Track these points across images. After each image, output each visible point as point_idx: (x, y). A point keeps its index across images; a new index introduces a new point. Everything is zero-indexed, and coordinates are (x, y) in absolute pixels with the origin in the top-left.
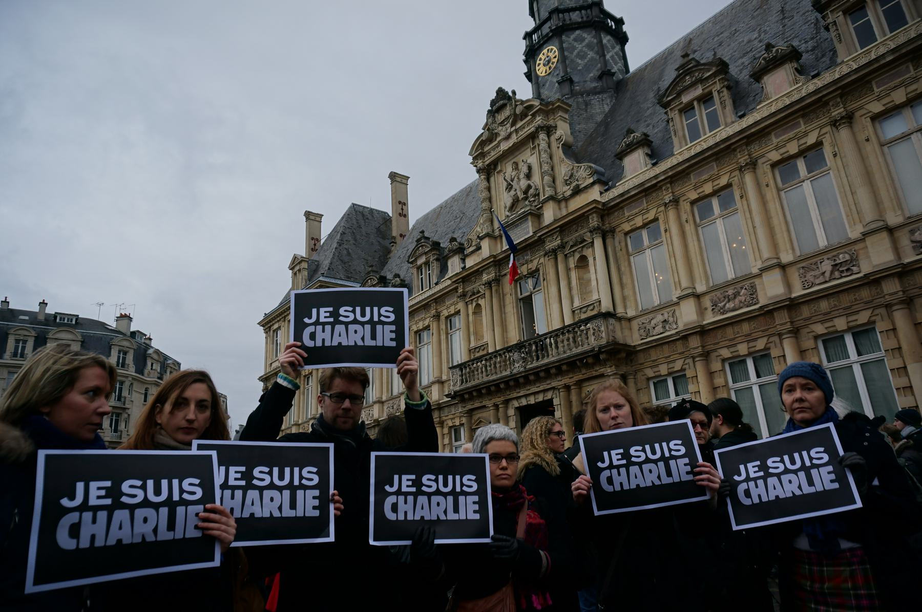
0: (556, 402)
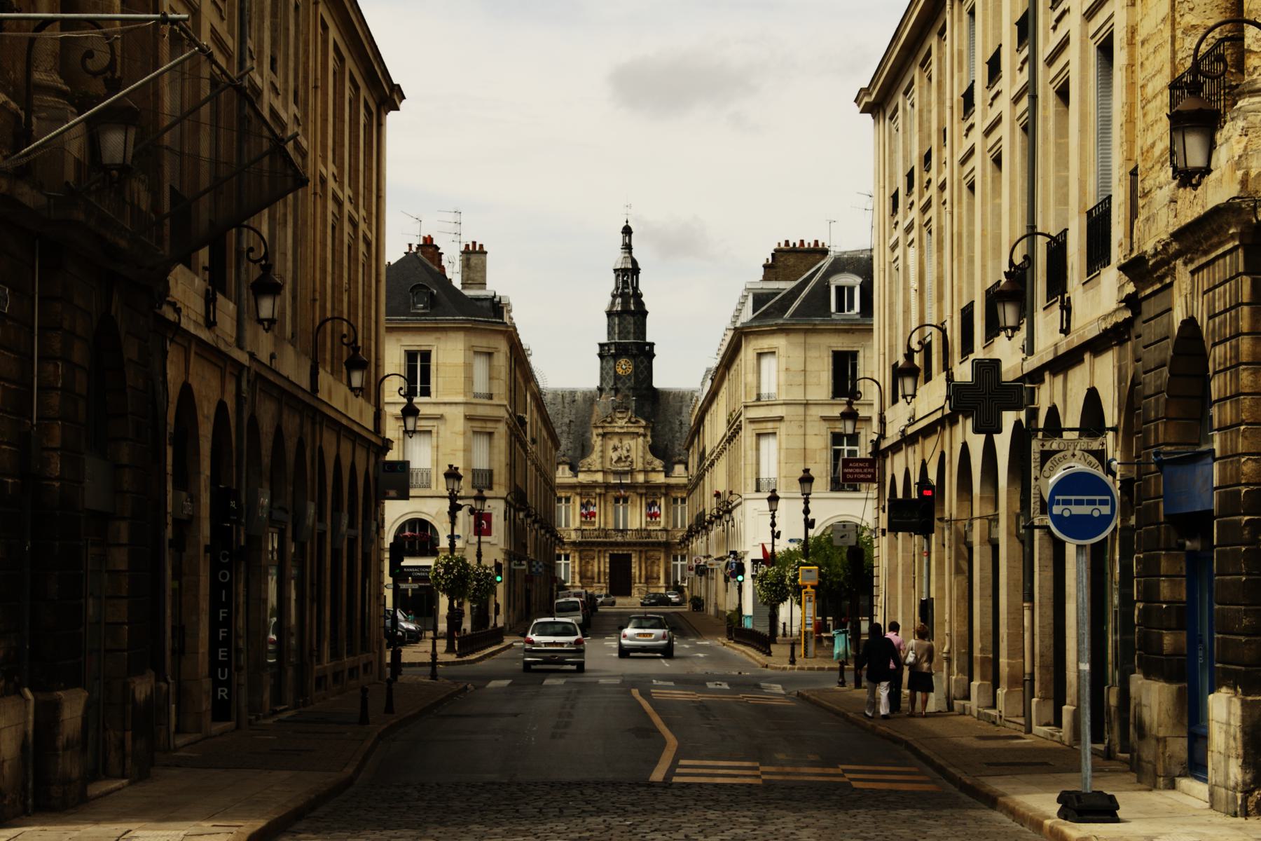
0: (633, 555)
